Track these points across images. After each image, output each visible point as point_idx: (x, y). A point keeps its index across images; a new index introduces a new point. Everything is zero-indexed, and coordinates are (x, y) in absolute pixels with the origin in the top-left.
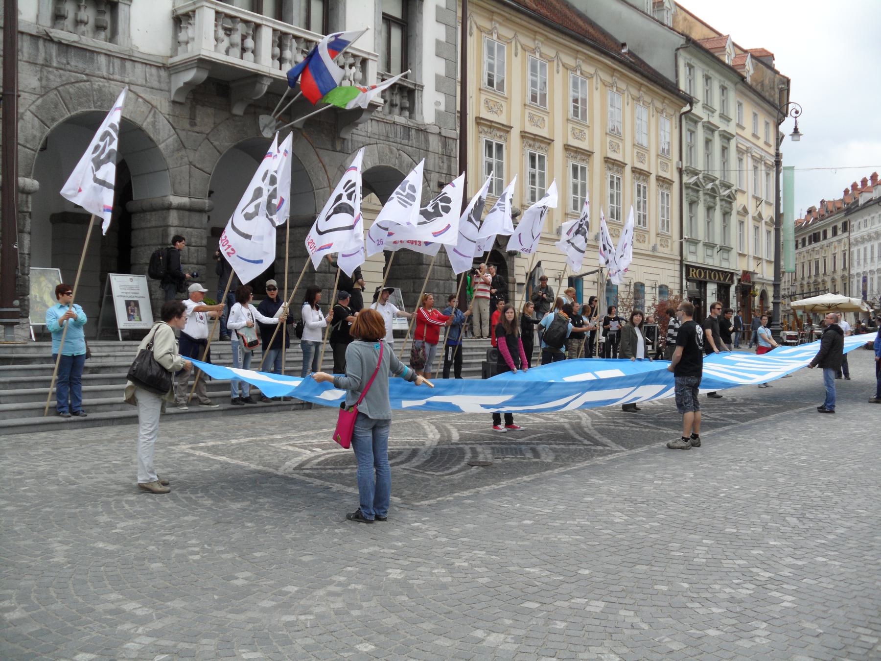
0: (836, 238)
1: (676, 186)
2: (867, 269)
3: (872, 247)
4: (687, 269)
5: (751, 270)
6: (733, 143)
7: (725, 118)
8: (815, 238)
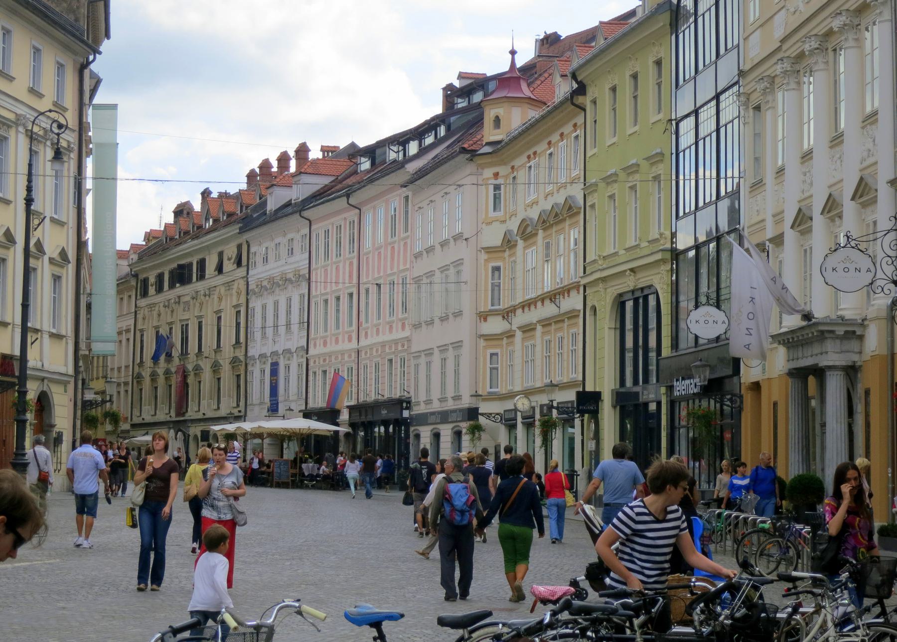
0: (221, 279)
2: (279, 348)
8: (181, 276)
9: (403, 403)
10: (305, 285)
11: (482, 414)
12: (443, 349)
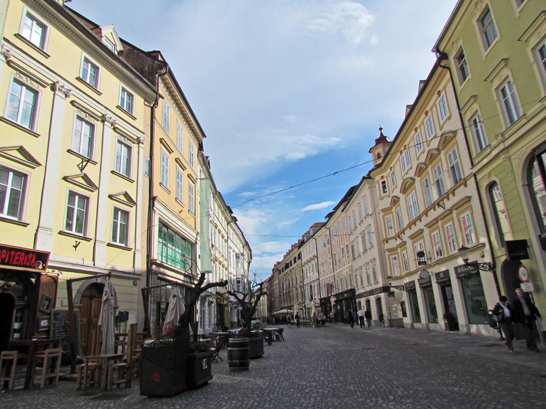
0: (296, 264)
2: (311, 280)
9: (353, 291)
10: (316, 259)
11: (393, 287)
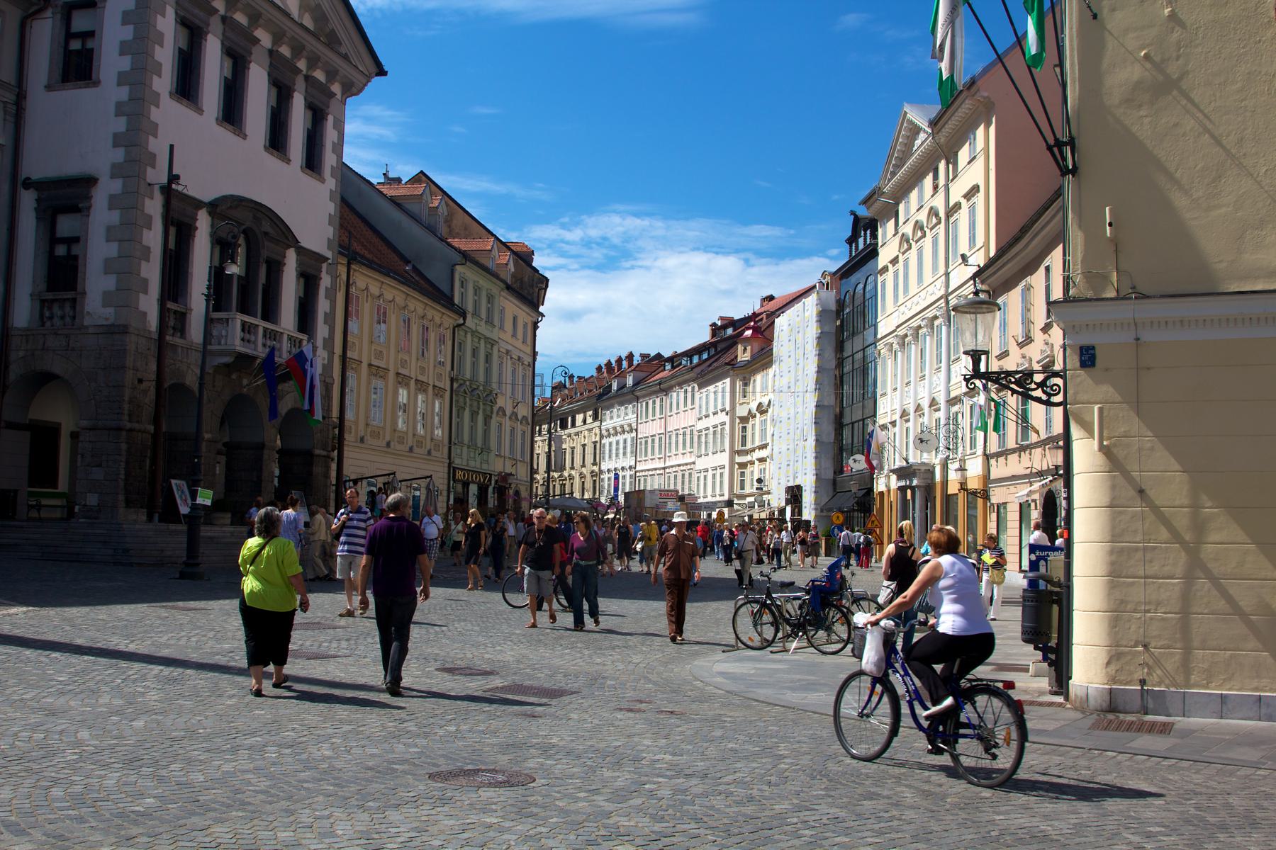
1: (447, 394)
2: (619, 466)
3: (625, 441)
4: (452, 469)
5: (508, 470)
6: (495, 348)
7: (489, 321)
12: (715, 469)
